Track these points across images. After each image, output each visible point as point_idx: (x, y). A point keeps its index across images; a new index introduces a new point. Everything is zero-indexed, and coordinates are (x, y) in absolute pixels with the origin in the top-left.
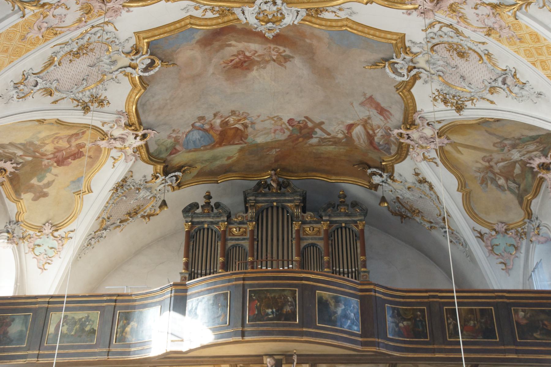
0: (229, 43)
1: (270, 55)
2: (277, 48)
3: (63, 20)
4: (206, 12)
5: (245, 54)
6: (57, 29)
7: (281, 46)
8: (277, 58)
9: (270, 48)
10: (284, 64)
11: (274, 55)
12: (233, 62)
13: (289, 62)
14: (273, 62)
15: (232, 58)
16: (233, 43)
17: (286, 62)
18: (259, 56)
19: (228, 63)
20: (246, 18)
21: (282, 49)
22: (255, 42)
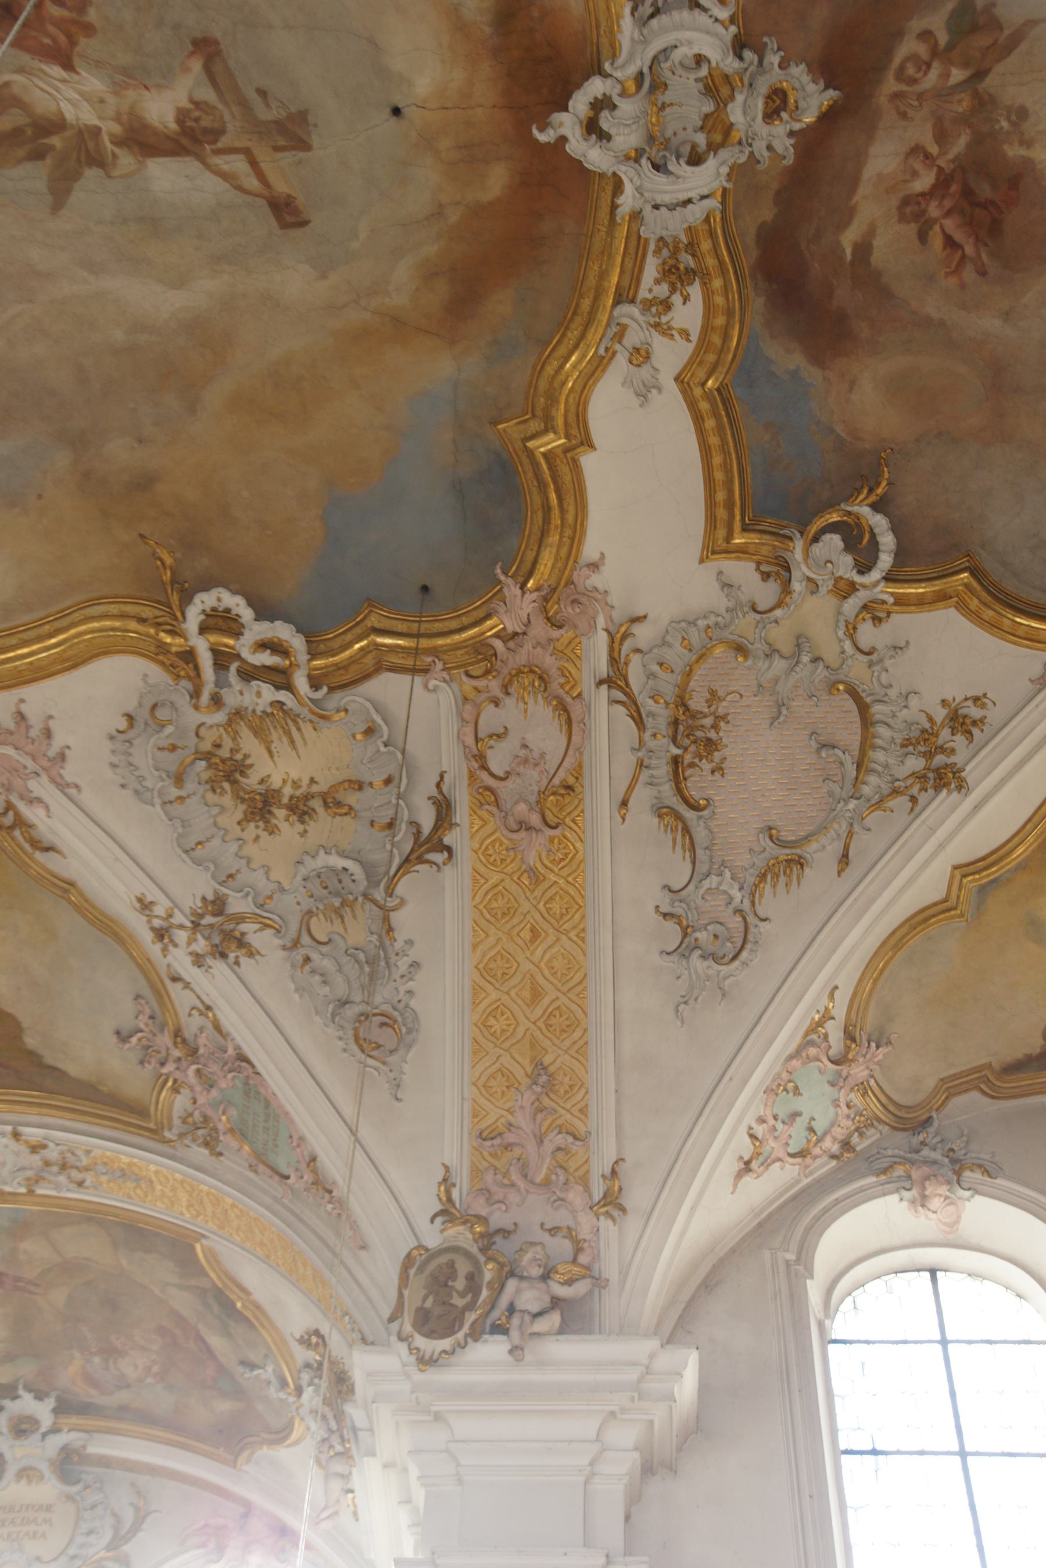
0: (848, 251)
1: (944, 94)
2: (902, 69)
3: (536, 755)
4: (670, 328)
5: (922, 194)
6: (556, 781)
7: (888, 53)
8: (965, 64)
9: (897, 96)
10: (1007, 32)
11: (947, 75)
12: (958, 236)
13: (999, 11)
14: (990, 83)
15: (937, 241)
16: (849, 239)
17: (996, 24)
18: (941, 136)
19: (964, 257)
20: (703, 197)
21: (909, 46)
22: (860, 158)
